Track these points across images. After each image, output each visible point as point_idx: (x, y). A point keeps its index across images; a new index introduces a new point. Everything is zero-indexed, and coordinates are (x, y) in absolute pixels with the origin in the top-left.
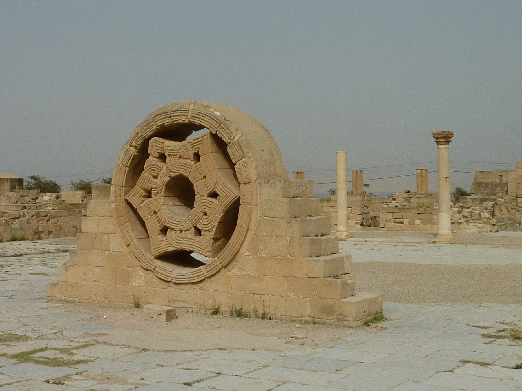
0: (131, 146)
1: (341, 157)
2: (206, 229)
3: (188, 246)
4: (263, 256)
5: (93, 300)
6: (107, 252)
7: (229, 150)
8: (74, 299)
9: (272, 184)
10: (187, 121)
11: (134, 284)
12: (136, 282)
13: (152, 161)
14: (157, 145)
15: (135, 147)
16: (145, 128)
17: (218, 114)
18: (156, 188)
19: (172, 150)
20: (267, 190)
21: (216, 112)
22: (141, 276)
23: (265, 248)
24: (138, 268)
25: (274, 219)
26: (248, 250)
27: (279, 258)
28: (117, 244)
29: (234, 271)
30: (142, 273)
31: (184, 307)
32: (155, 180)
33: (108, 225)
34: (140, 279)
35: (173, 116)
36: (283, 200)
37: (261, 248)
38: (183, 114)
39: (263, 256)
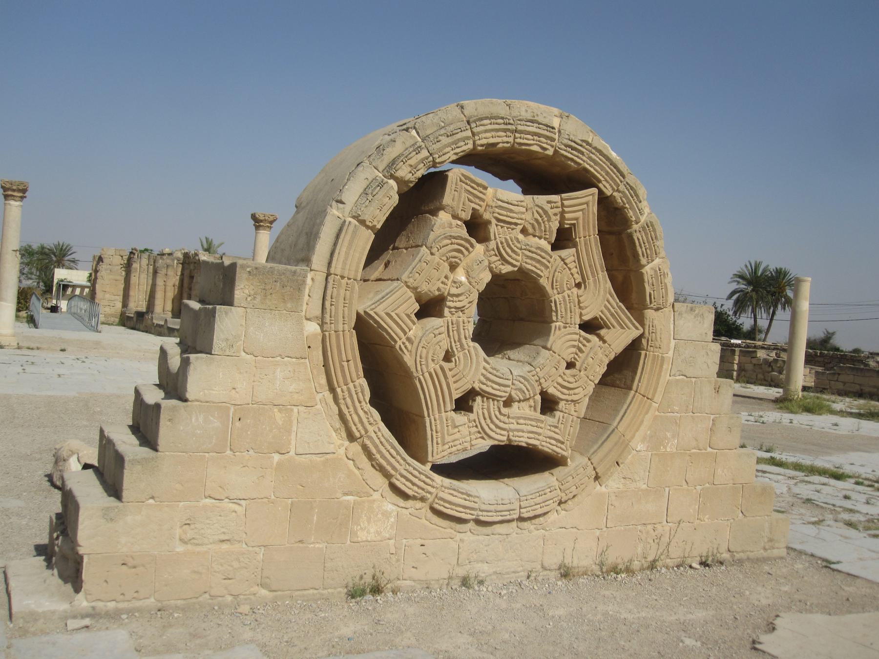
2: (570, 398)
3: (526, 435)
4: (668, 450)
5: (212, 597)
6: (276, 457)
10: (550, 152)
11: (362, 536)
12: (368, 531)
13: (444, 224)
14: (465, 190)
18: (458, 295)
19: (511, 211)
22: (386, 514)
23: (673, 437)
24: (376, 496)
25: (693, 380)
26: (643, 440)
27: (694, 453)
30: (390, 507)
35: (521, 132)
37: (668, 434)
38: (545, 133)
39: (668, 450)
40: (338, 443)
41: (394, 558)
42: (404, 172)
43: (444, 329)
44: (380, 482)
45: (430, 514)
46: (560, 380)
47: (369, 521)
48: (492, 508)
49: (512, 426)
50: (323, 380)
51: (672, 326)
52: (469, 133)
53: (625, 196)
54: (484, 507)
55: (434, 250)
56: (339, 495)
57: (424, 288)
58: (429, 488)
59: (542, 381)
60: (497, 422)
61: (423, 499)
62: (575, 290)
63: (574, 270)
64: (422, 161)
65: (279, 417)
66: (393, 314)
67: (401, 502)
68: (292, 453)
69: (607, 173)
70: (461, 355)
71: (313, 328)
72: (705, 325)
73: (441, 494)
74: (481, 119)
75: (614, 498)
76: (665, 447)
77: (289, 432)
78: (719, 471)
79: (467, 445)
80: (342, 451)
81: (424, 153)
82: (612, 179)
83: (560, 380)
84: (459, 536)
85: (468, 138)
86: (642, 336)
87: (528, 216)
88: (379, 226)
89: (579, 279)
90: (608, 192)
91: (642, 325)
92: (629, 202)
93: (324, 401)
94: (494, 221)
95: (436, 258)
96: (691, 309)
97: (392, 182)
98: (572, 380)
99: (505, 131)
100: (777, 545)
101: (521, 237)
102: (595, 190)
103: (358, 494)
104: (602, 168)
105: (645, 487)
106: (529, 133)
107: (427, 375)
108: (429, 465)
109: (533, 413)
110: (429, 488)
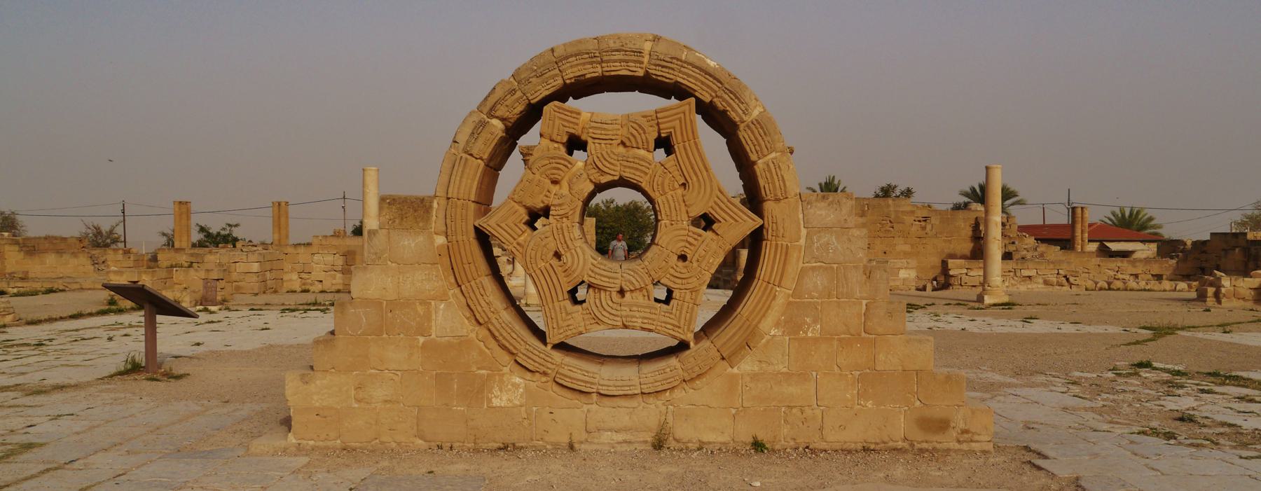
0: (491, 116)
1: (371, 177)
4: (810, 335)
5: (382, 443)
6: (422, 340)
7: (743, 134)
8: (329, 443)
9: (832, 203)
10: (641, 73)
11: (496, 402)
15: (503, 119)
16: (534, 80)
17: (712, 64)
18: (560, 205)
20: (823, 212)
21: (708, 61)
22: (516, 386)
23: (815, 321)
24: (506, 370)
26: (777, 325)
28: (448, 320)
29: (747, 365)
30: (517, 380)
31: (625, 442)
32: (555, 189)
33: (426, 281)
34: (510, 392)
35: (608, 61)
36: (856, 232)
40: (467, 328)
41: (526, 422)
42: (502, 111)
43: (549, 234)
44: (506, 358)
45: (556, 388)
46: (672, 271)
47: (501, 391)
48: (611, 383)
49: (624, 313)
50: (453, 280)
51: (801, 216)
52: (557, 71)
53: (724, 100)
54: (602, 382)
55: (535, 170)
56: (474, 369)
57: (529, 203)
58: (549, 365)
59: (652, 273)
60: (609, 309)
61: (545, 374)
62: (680, 191)
63: (676, 173)
64: (517, 100)
65: (420, 310)
66: (503, 225)
67: (529, 375)
68: (433, 336)
69: (703, 83)
70: (568, 255)
71: (440, 240)
72: (844, 211)
73: (561, 371)
74: (567, 58)
75: (748, 379)
76: (806, 333)
77: (429, 320)
78: (881, 357)
79: (581, 329)
80: (473, 335)
81: (519, 94)
82: (708, 86)
83: (672, 271)
84: (585, 408)
85: (556, 75)
86: (762, 227)
87: (624, 131)
88: (486, 156)
89: (683, 181)
90: (707, 99)
91: (761, 216)
92: (729, 105)
93: (454, 295)
94: (590, 141)
95: (538, 176)
96: (823, 197)
97: (495, 122)
98: (684, 271)
99: (591, 63)
100: (976, 438)
101: (621, 149)
102: (693, 99)
103: (490, 369)
104: (696, 79)
105: (785, 370)
106: (615, 61)
107: (538, 272)
108: (549, 347)
109: (646, 301)
110: (549, 365)
